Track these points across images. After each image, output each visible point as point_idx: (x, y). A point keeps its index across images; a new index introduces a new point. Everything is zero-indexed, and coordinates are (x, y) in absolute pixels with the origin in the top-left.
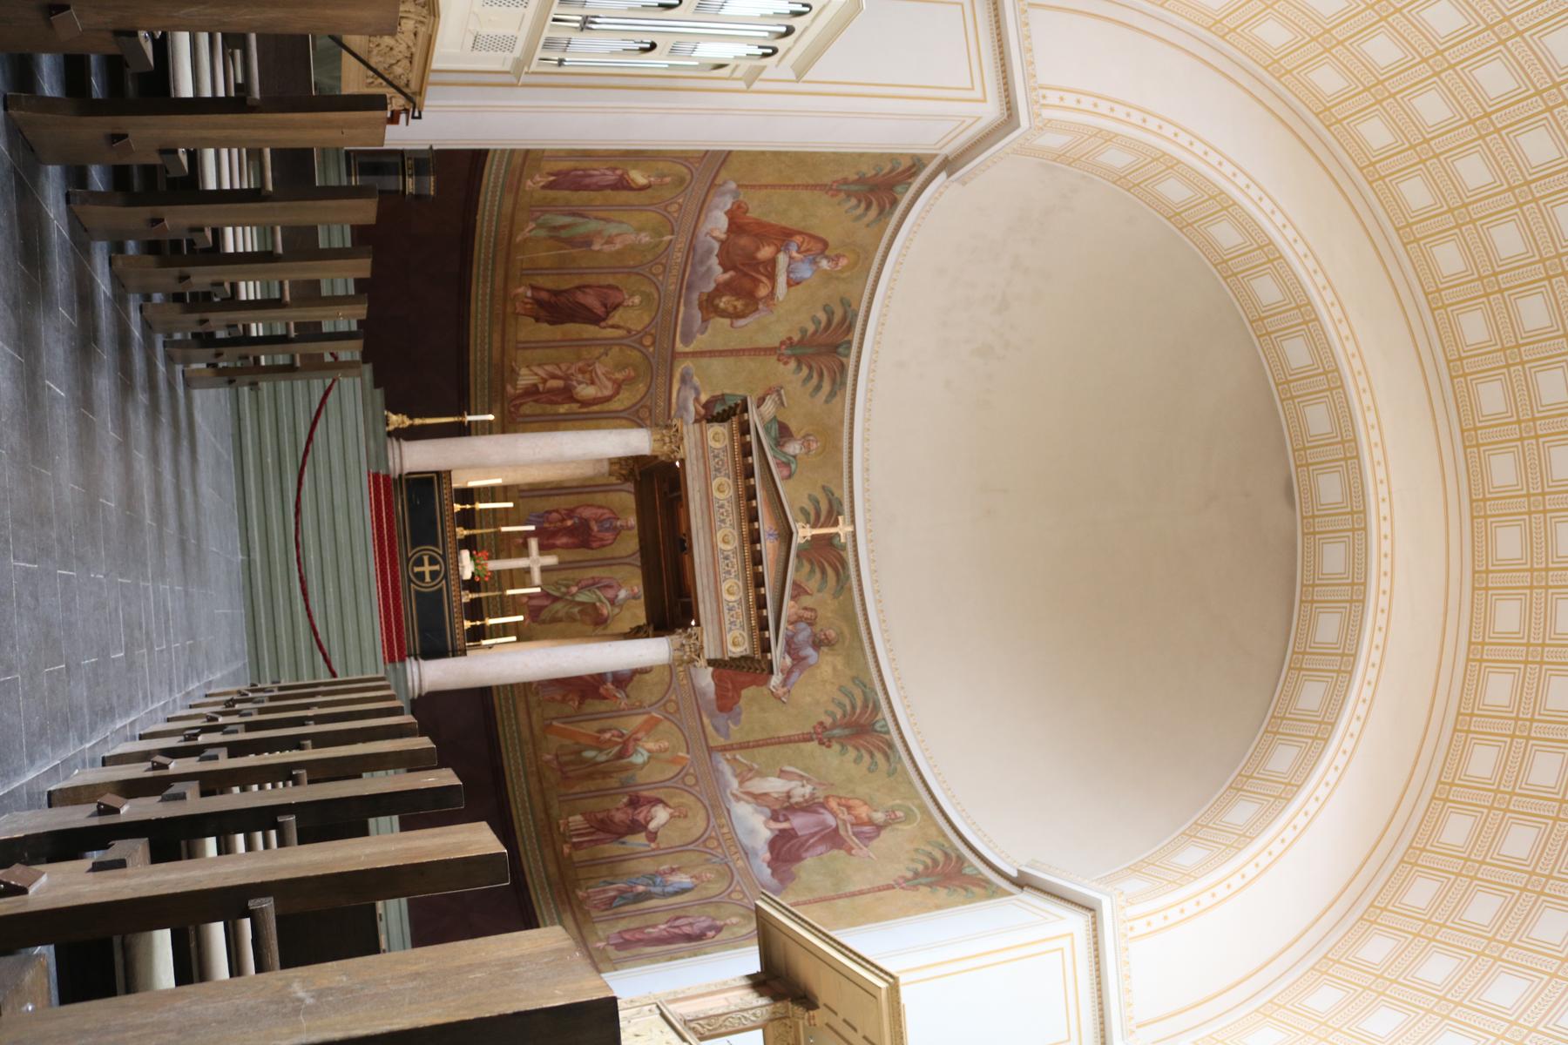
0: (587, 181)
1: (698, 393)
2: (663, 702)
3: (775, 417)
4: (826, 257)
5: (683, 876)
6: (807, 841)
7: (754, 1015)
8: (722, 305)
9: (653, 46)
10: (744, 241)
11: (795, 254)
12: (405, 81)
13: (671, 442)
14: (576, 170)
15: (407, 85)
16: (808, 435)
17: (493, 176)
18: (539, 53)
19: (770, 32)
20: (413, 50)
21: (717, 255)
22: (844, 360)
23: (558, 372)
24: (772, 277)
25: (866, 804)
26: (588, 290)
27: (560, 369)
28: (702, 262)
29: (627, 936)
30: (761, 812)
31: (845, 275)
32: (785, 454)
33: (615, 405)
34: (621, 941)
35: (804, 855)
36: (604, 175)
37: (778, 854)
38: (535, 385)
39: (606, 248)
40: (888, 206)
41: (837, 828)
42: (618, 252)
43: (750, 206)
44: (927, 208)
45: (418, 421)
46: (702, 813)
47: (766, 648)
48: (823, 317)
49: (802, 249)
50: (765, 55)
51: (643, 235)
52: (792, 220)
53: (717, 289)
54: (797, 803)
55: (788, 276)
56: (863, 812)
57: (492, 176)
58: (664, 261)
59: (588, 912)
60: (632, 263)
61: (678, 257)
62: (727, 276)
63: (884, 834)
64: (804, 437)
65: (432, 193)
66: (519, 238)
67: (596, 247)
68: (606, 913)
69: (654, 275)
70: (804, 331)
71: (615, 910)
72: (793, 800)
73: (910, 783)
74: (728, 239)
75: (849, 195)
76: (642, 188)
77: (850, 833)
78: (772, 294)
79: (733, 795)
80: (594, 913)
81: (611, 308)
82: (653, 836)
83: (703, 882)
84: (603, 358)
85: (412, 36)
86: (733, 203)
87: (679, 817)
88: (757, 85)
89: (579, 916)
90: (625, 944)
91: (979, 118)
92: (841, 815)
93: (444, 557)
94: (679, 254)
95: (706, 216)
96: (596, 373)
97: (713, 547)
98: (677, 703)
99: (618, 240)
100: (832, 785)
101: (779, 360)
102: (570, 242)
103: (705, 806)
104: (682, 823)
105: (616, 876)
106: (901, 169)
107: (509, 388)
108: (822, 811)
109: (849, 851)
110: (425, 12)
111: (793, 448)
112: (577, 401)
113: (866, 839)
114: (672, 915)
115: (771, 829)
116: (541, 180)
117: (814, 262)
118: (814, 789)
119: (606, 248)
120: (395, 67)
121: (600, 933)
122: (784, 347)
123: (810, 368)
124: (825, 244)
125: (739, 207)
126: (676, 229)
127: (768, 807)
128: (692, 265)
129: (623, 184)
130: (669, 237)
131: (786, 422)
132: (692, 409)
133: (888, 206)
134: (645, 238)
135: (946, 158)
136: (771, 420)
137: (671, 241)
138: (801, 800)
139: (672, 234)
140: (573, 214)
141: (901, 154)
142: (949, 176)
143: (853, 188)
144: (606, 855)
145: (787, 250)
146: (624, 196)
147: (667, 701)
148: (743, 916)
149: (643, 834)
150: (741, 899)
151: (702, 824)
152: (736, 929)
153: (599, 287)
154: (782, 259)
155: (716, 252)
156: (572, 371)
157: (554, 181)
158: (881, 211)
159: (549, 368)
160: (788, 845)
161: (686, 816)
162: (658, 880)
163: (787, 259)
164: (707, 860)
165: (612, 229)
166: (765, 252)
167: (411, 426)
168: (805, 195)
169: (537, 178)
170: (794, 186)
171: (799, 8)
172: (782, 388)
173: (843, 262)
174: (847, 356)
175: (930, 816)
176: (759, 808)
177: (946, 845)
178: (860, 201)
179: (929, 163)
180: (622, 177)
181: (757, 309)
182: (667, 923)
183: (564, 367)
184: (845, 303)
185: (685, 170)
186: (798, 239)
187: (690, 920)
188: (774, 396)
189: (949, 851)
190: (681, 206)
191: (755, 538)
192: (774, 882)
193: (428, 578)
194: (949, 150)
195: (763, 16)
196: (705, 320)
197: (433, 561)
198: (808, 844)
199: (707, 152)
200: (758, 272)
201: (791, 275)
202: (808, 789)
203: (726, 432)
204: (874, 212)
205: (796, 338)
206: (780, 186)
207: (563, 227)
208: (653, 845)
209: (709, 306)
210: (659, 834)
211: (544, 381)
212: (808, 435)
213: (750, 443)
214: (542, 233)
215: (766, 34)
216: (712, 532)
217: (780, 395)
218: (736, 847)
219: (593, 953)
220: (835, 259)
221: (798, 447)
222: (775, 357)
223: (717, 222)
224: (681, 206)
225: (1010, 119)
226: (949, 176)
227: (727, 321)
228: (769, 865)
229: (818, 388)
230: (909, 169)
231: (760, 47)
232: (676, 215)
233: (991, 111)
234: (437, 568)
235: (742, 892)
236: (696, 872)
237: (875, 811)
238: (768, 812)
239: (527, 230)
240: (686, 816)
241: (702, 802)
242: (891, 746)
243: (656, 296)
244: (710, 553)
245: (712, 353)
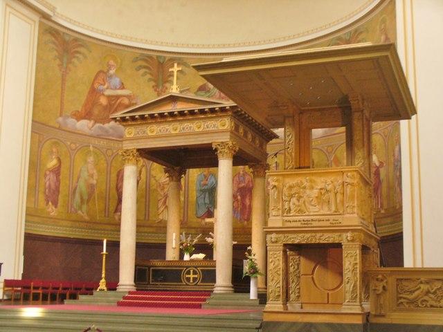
0: (53, 186)
2: (327, 154)
4: (108, 71)
7: (289, 136)
10: (96, 111)
11: (106, 86)
23: (163, 200)
24: (118, 97)
26: (119, 186)
28: (107, 131)
31: (119, 61)
39: (95, 177)
42: (99, 171)
43: (74, 110)
45: (103, 275)
47: (223, 110)
48: (142, 71)
49: (102, 82)
52: (84, 90)
55: (119, 89)
58: (105, 150)
60: (105, 165)
61: (102, 143)
69: (112, 155)
70: (150, 80)
74: (94, 120)
76: (59, 161)
78: (128, 97)
84: (157, 179)
93: (187, 267)
97: (177, 135)
98: (328, 146)
99: (91, 172)
102: (90, 195)
106: (53, 39)
116: (51, 208)
117: (111, 77)
119: (94, 178)
125: (75, 115)
126: (85, 145)
128: (110, 135)
129: (57, 171)
130: (91, 148)
131: (198, 87)
134: (91, 159)
143: (65, 60)
146: (64, 171)
147: (327, 151)
149: (381, 169)
153: (118, 180)
154: (108, 92)
155: (101, 125)
156: (162, 193)
157: (52, 202)
158: (82, 46)
159: (160, 204)
162: (396, 164)
163: (108, 90)
165: (85, 175)
167: (106, 279)
168: (68, 84)
170: (62, 90)
173: (112, 62)
174: (165, 58)
178: (74, 57)
183: (160, 198)
186: (96, 86)
191: (171, 114)
193: (196, 276)
194: (36, 18)
197: (188, 273)
200: (114, 104)
204: (82, 50)
205: (154, 84)
214: (85, 207)
216: (171, 136)
220: (110, 67)
223: (84, 125)
230: (53, 35)
234: (192, 271)
242: (356, 31)
244: (191, 136)
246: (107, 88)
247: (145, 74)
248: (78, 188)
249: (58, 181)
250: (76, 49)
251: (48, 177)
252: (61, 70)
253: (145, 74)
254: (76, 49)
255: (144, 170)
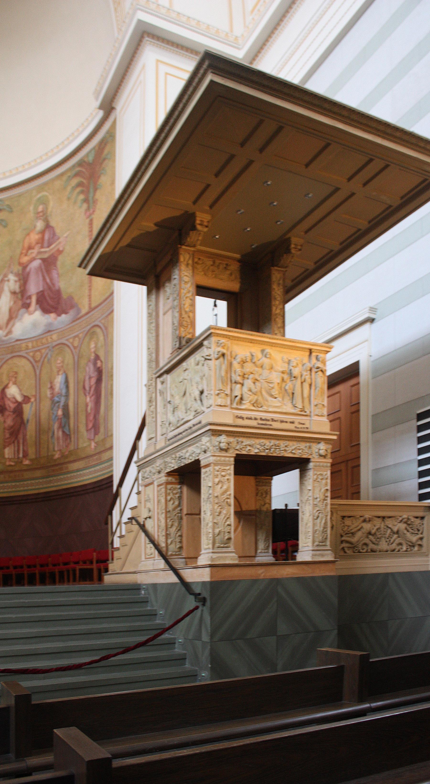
5: (56, 381)
6: (47, 284)
25: (28, 234)
29: (90, 425)
30: (22, 316)
34: (93, 430)
35: (57, 288)
37: (53, 307)
41: (43, 260)
46: (16, 360)
54: (20, 287)
56: (34, 237)
59: (69, 451)
63: (53, 223)
68: (72, 439)
71: (72, 432)
72: (18, 290)
73: (20, 195)
77: (47, 249)
79: (7, 335)
80: (72, 447)
82: (26, 399)
83: (62, 366)
87: (16, 378)
89: (72, 459)
90: (96, 428)
92: (34, 255)
100: (11, 258)
103: (12, 358)
104: (21, 376)
105: (49, 429)
108: (28, 269)
109: (60, 252)
113: (54, 237)
114: (81, 392)
115: (35, 310)
118: (12, 272)
121: (85, 445)
127: (19, 310)
138: (18, 284)
144: (34, 435)
148: (91, 339)
149: (24, 406)
150: (80, 339)
151: (23, 362)
152: (99, 345)
160: (48, 298)
161: (16, 373)
164: (49, 360)
175: (46, 184)
176: (19, 317)
177: (69, 174)
182: (86, 395)
187: (87, 378)
189: (74, 172)
192: (72, 313)
198: (50, 284)
202: (12, 277)
208: (33, 400)
210: (25, 394)
218: (43, 338)
219: (98, 451)
228: (59, 315)
235: (75, 337)
236: (55, 370)
237: (35, 227)
238: (23, 310)
240: (16, 373)
241: (8, 360)
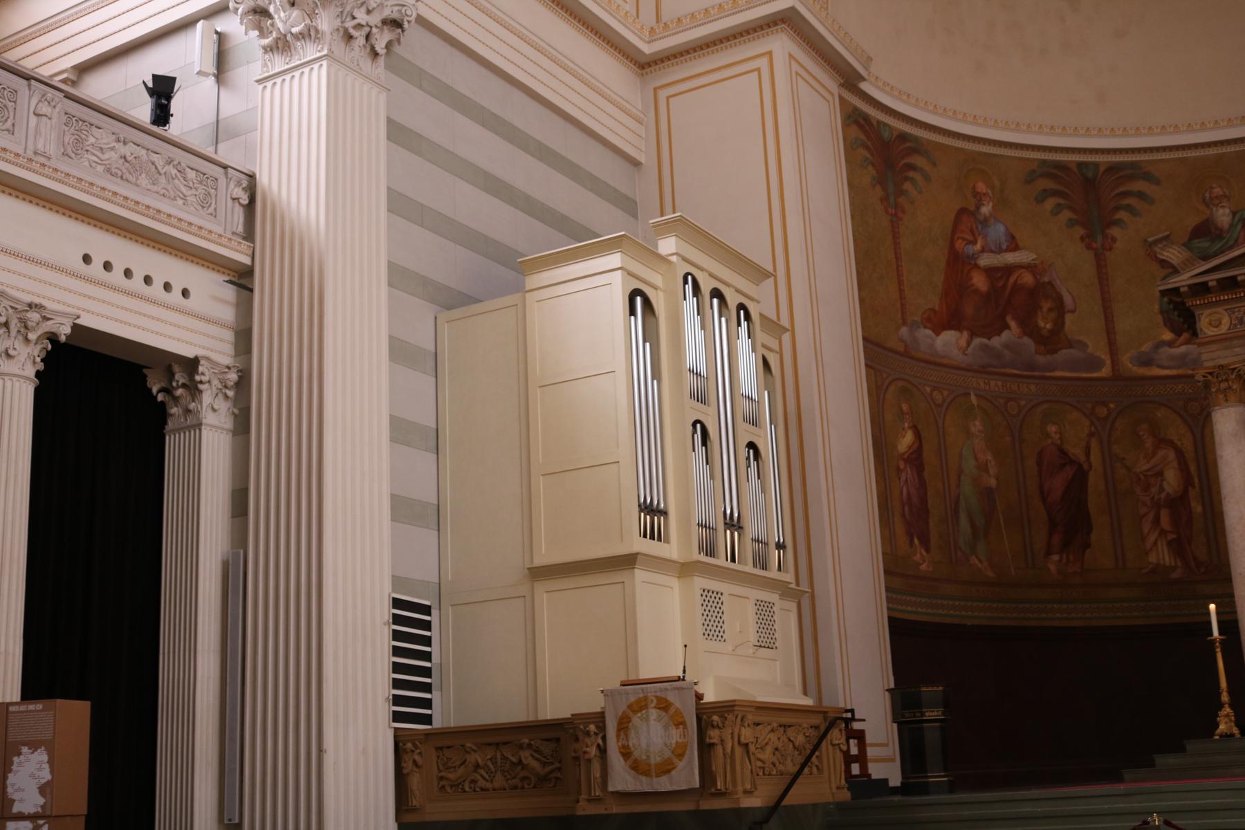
1: (1163, 343)
3: (1184, 245)
4: (978, 208)
8: (1049, 326)
9: (751, 445)
11: (978, 247)
12: (810, 730)
13: (1227, 380)
14: (903, 515)
15: (817, 727)
16: (1204, 200)
17: (919, 610)
18: (773, 573)
19: (720, 316)
20: (775, 725)
21: (989, 339)
22: (1102, 169)
24: (1009, 269)
27: (1146, 514)
32: (1231, 226)
33: (1187, 444)
36: (906, 480)
38: (1169, 543)
40: (908, 144)
44: (905, 97)
45: (1225, 697)
48: (1050, 203)
49: (970, 238)
50: (748, 317)
51: (973, 429)
53: (1030, 336)
55: (1006, 251)
57: (919, 611)
58: (1002, 401)
62: (1013, 324)
64: (1207, 206)
65: (940, 688)
66: (990, 574)
67: (993, 482)
70: (1071, 223)
75: (900, 192)
76: (918, 435)
78: (1030, 267)
81: (1065, 459)
85: (760, 727)
86: (925, 327)
88: (785, 322)
91: (790, 55)
94: (993, 383)
95: (943, 357)
96: (1145, 471)
101: (1111, 249)
106: (862, 136)
107: (1175, 575)
110: (730, 717)
111: (1223, 216)
112: (1186, 491)
116: (919, 554)
117: (985, 222)
119: (992, 471)
120: (797, 744)
122: (1094, 245)
123: (1117, 209)
124: (962, 211)
129: (916, 458)
130: (973, 397)
131: (1190, 229)
132: (1183, 349)
133: (908, 144)
134: (976, 426)
135: (842, 85)
136: (1190, 249)
137: (976, 395)
139: (968, 394)
140: (956, 512)
141: (845, 139)
142: (863, 79)
145: (974, 257)
154: (986, 260)
155: (985, 341)
157: (919, 539)
163: (985, 255)
165: (970, 465)
166: (979, 282)
167: (1231, 706)
169: (917, 557)
171: (689, 288)
172: (1145, 241)
173: (981, 187)
178: (907, 179)
179: (851, 104)
180: (907, 461)
181: (1050, 283)
184: (1031, 178)
185: (892, 388)
186: (959, 245)
188: (1157, 249)
190: (934, 389)
194: (833, 86)
195: (703, 327)
196: (1070, 345)
199: (866, 365)
201: (1004, 247)
203: (1207, 312)
204: (919, 161)
205: (1082, 231)
206: (899, 275)
207: (973, 525)
209: (1052, 341)
211: (1163, 532)
212: (1204, 200)
213: (1218, 281)
215: (723, 319)
217: (1155, 242)
220: (979, 198)
221: (1221, 211)
222: (1107, 253)
223: (949, 342)
224: (934, 389)
225: (787, 20)
226: (863, 79)
227: (1069, 318)
229: (1141, 195)
230: (861, 127)
231: (739, 324)
232: (946, 393)
233: (781, 45)
239: (980, 565)
243: (1045, 406)
245: (1110, 331)
246: (983, 250)
247: (1057, 210)
248: (961, 497)
249: (922, 485)
250: (905, 161)
251: (903, 478)
252: (887, 212)
253: (1057, 210)
254: (905, 161)
255: (1094, 444)
